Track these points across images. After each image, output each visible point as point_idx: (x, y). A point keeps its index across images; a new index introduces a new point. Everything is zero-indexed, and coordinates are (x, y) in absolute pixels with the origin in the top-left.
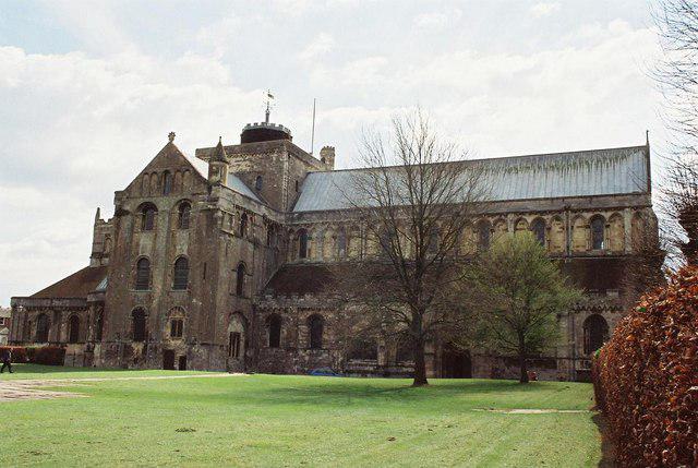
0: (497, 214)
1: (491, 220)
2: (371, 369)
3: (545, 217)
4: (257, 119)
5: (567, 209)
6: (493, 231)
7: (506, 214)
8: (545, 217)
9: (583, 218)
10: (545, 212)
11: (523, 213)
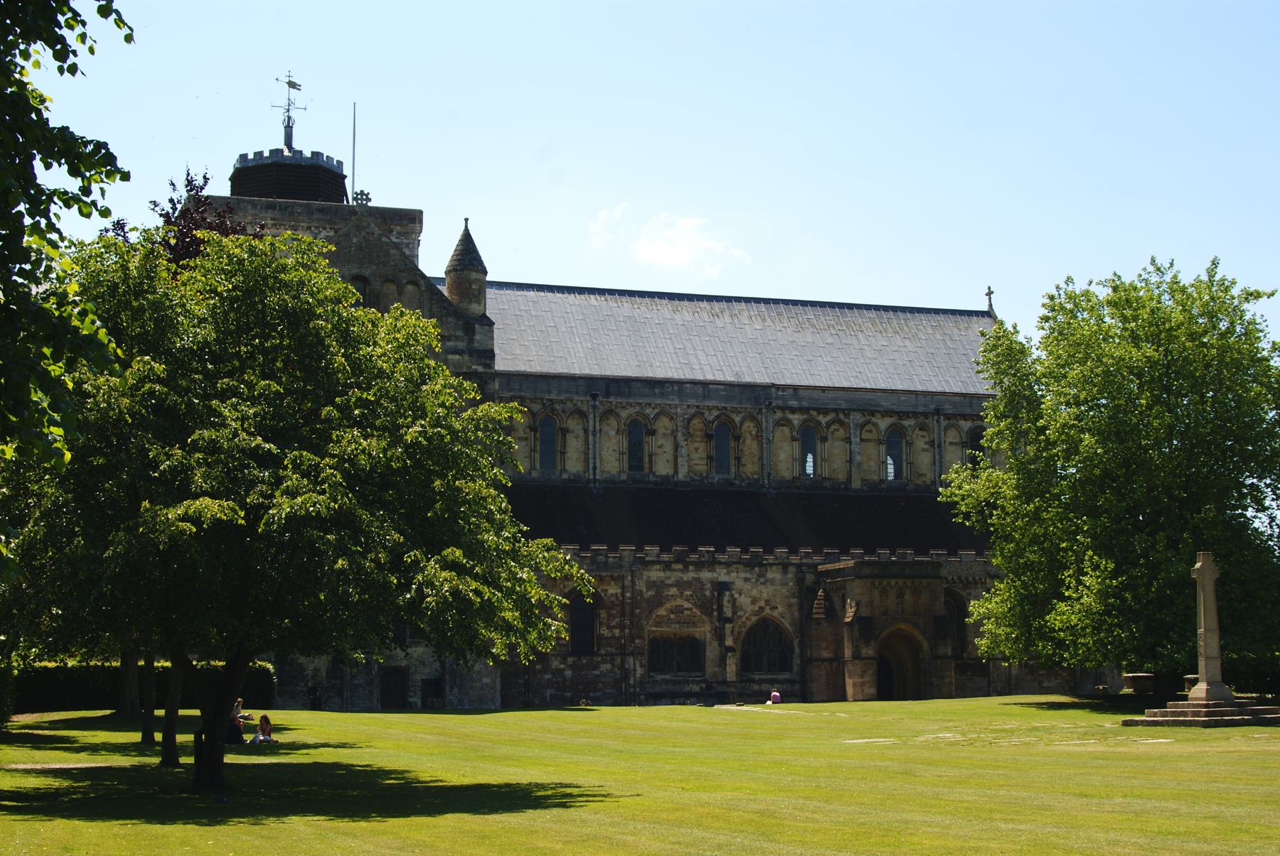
0: (834, 410)
1: (823, 420)
2: (696, 688)
3: (906, 423)
4: (268, 141)
5: (938, 411)
6: (824, 439)
7: (847, 412)
8: (906, 423)
9: (959, 429)
10: (906, 415)
11: (873, 413)
